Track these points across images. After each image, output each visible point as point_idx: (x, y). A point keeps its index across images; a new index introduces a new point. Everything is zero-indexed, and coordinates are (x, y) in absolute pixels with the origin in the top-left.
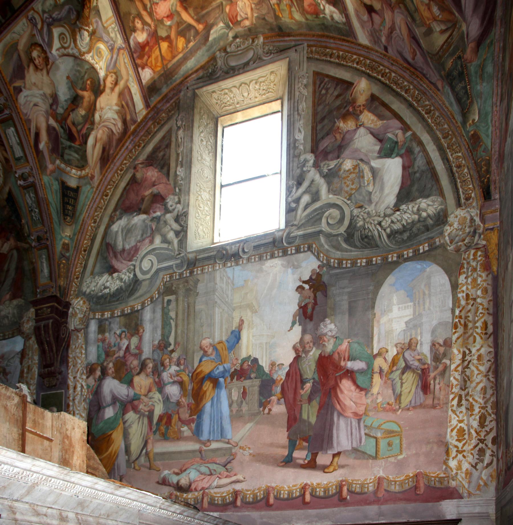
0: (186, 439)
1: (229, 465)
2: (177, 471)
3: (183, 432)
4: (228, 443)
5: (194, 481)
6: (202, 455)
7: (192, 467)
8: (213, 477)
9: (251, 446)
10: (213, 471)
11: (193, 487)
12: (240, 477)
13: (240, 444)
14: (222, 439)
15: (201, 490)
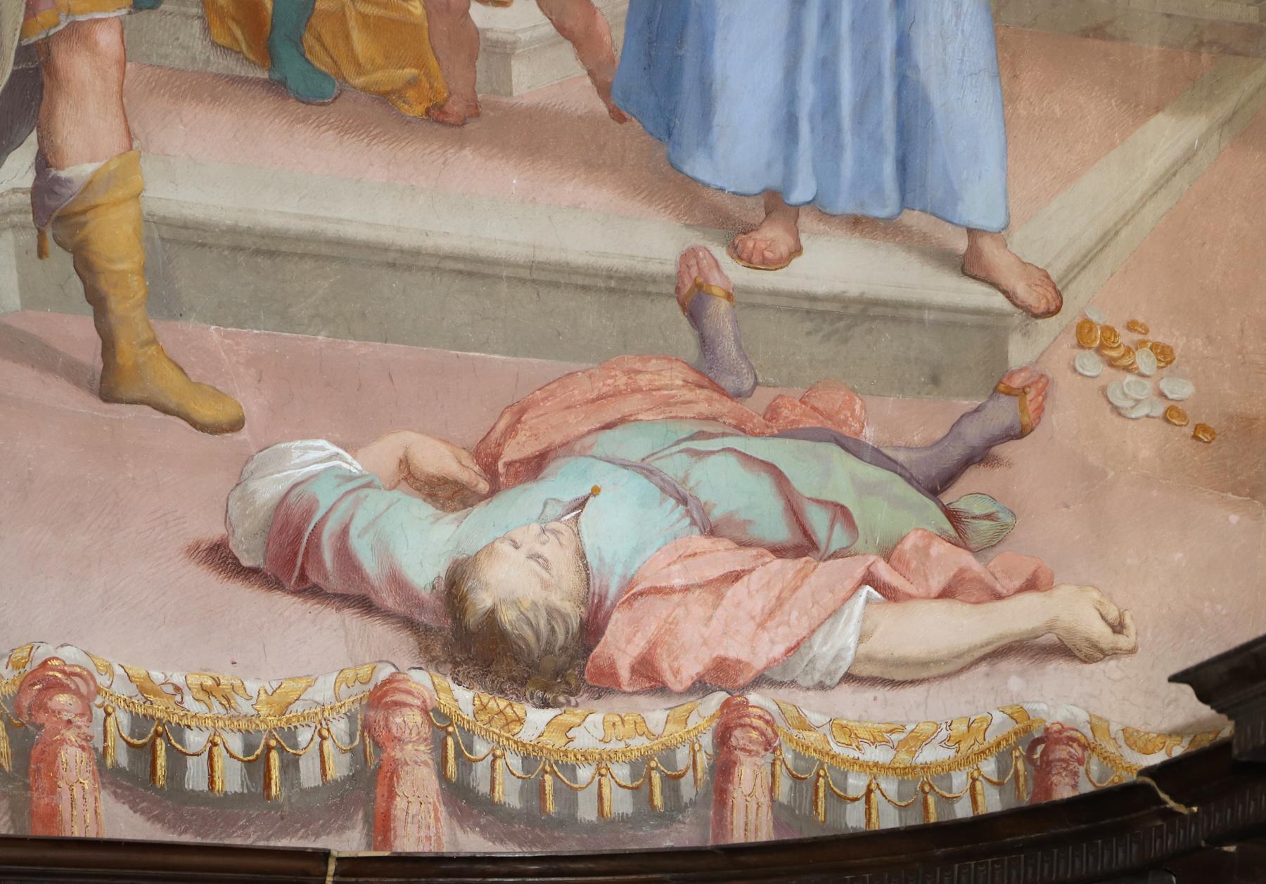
0: (533, 137)
1: (973, 479)
2: (437, 458)
3: (504, 51)
4: (969, 266)
5: (634, 594)
6: (705, 343)
7: (609, 442)
8: (824, 574)
9: (1178, 343)
10: (818, 520)
11: (621, 645)
12: (1074, 609)
13: (1082, 299)
14: (914, 219)
15: (701, 687)
